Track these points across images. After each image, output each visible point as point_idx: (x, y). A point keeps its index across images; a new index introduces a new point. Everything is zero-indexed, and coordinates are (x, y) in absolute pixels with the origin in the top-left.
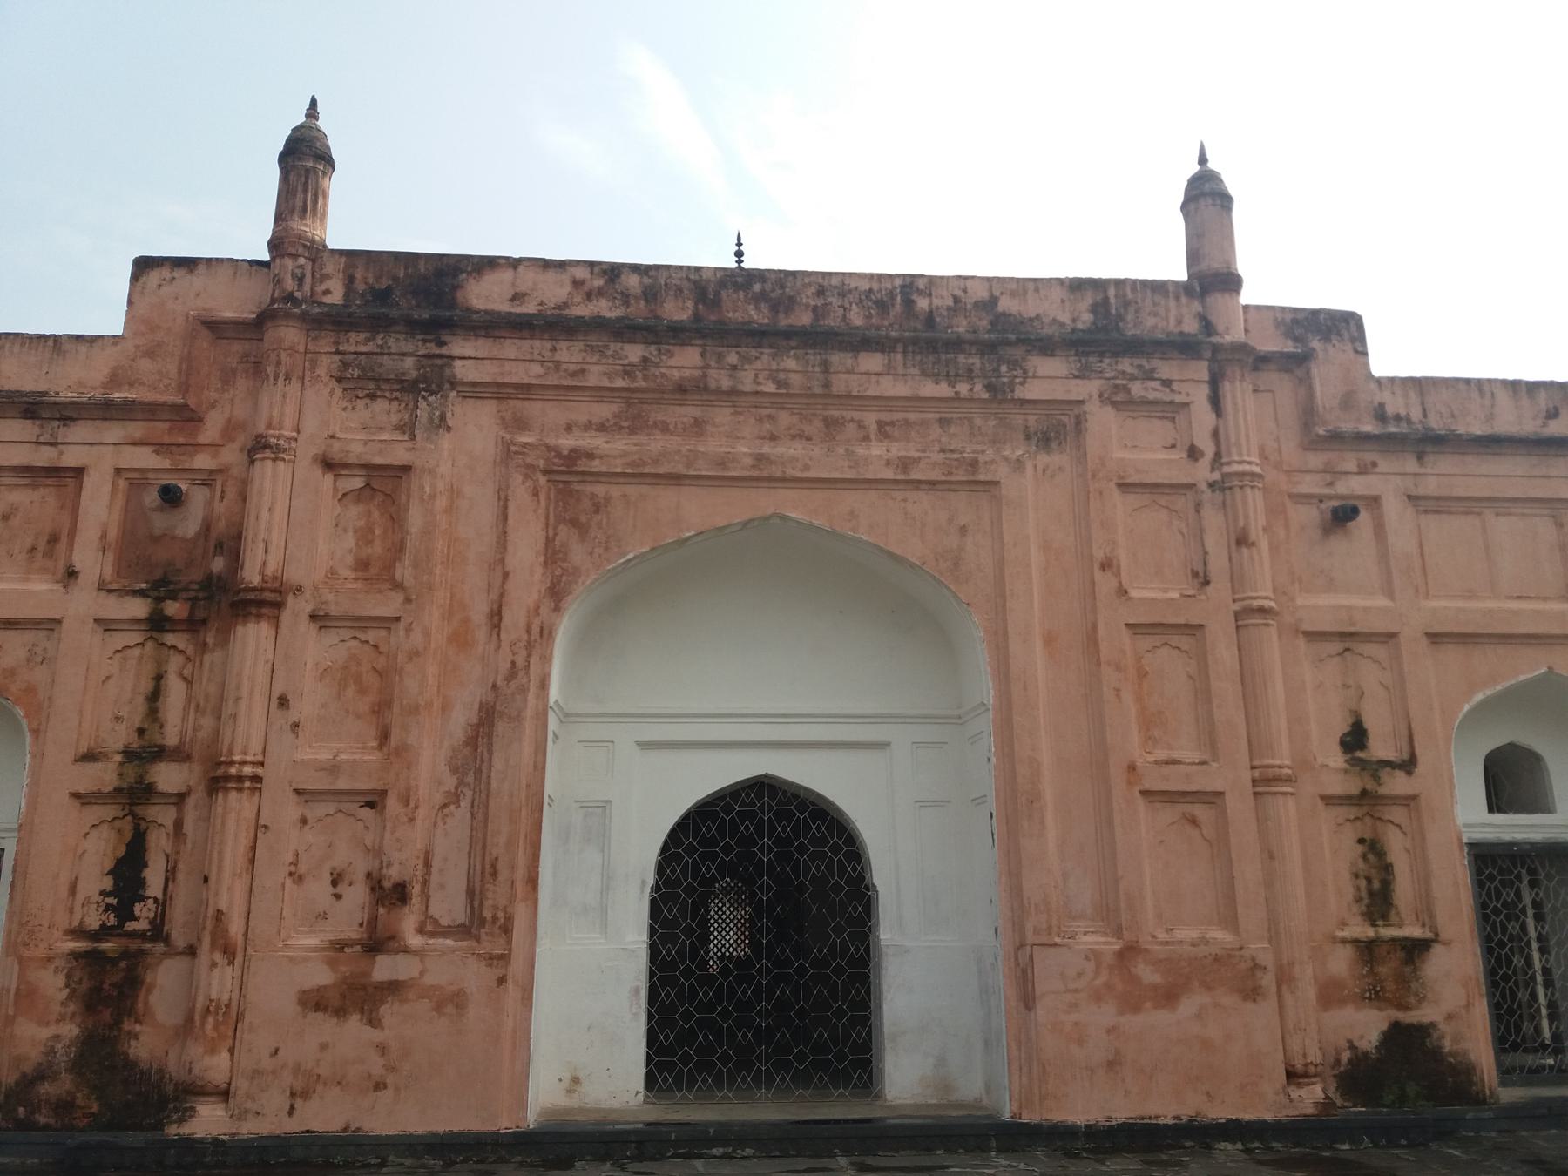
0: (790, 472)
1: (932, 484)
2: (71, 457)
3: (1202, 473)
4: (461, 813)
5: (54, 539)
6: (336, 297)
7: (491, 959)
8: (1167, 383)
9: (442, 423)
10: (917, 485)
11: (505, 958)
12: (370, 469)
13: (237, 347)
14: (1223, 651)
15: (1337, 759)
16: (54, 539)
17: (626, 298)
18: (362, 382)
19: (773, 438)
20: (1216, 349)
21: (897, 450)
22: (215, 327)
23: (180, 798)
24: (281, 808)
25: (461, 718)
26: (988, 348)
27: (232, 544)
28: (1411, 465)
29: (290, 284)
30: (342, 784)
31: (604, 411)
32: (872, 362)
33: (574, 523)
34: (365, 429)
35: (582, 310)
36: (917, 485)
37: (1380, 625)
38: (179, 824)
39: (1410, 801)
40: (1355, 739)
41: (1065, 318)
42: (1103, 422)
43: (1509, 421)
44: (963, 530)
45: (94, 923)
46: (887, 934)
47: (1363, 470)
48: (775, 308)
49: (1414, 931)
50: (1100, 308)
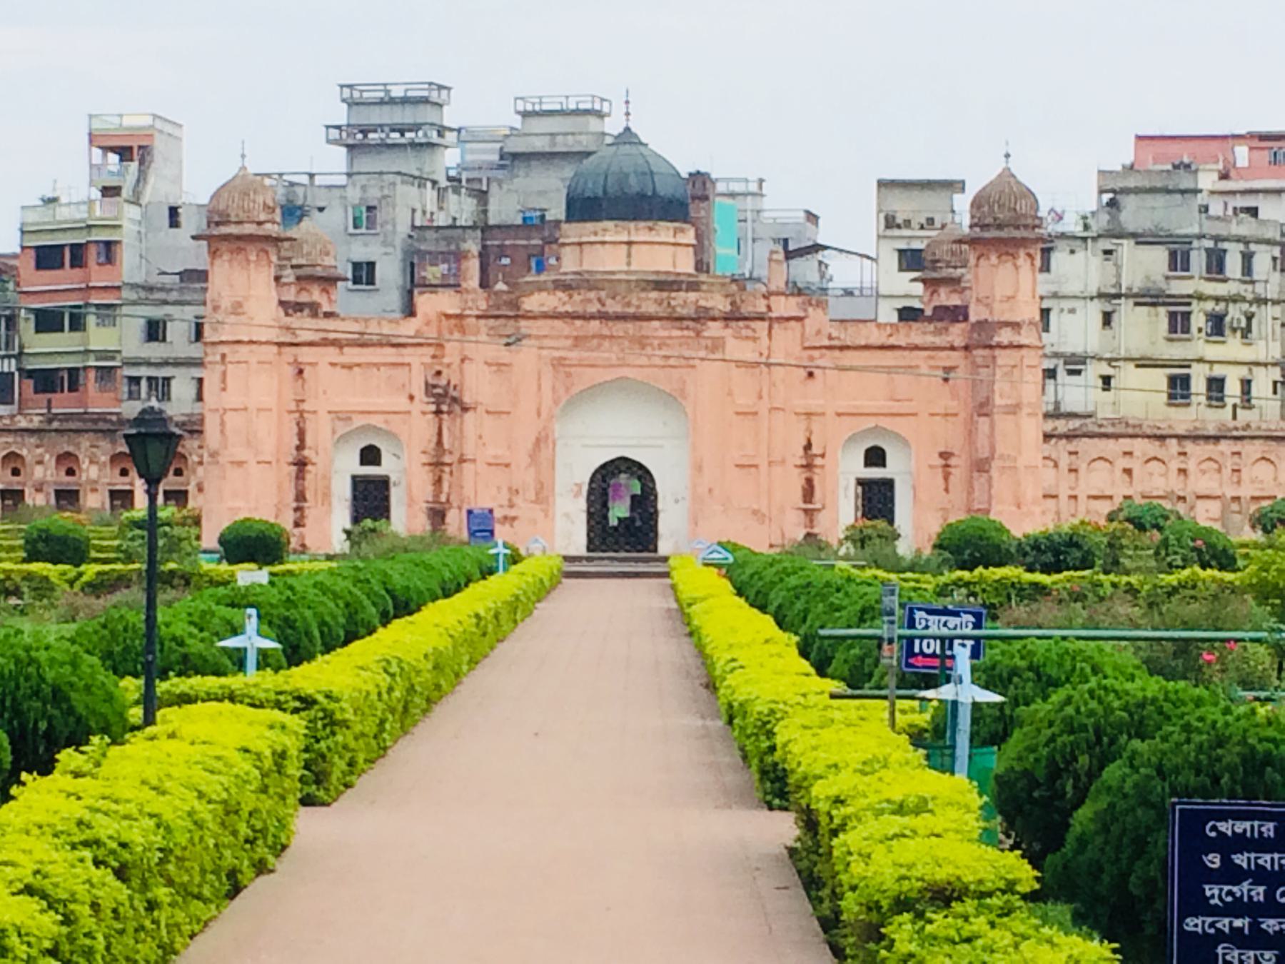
2: (406, 360)
4: (532, 470)
5: (404, 386)
7: (543, 510)
13: (453, 321)
15: (801, 452)
16: (404, 386)
18: (494, 334)
20: (771, 319)
22: (448, 316)
23: (450, 465)
24: (481, 466)
26: (693, 320)
28: (837, 353)
31: (569, 342)
32: (656, 324)
34: (496, 351)
35: (562, 309)
37: (820, 410)
38: (451, 473)
39: (822, 467)
40: (808, 446)
41: (721, 307)
46: (660, 506)
49: (818, 506)
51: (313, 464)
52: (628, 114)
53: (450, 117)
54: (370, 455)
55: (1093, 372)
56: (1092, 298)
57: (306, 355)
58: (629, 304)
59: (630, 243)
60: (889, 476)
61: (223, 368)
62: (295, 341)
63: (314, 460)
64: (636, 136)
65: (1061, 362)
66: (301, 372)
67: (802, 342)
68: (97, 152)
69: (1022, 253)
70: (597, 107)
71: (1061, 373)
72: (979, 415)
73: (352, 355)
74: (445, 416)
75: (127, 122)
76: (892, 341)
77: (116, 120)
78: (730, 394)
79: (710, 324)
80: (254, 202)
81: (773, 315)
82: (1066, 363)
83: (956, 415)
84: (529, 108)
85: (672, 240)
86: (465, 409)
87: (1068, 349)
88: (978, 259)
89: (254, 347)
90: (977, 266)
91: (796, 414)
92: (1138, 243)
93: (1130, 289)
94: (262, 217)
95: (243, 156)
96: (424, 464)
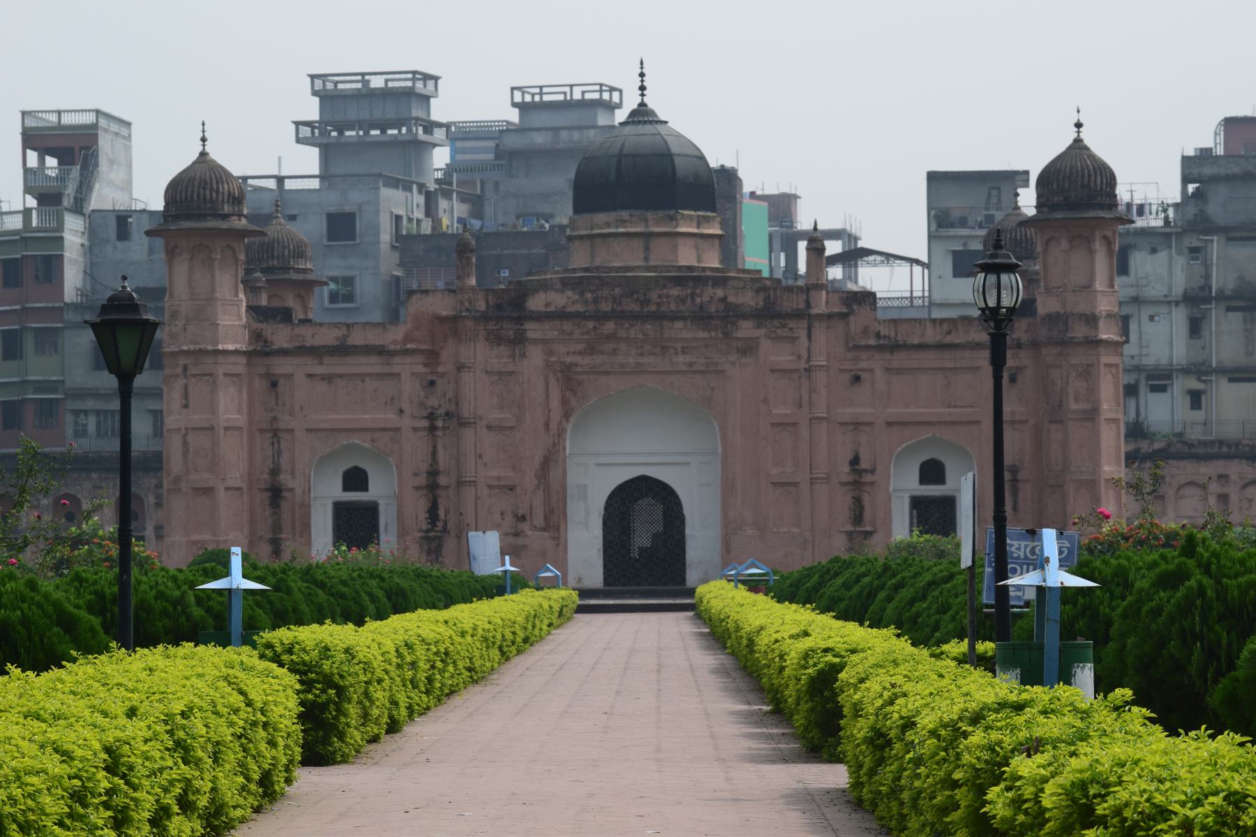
0: (649, 369)
1: (701, 372)
2: (396, 369)
3: (802, 365)
4: (540, 493)
6: (483, 308)
8: (791, 329)
9: (523, 355)
10: (696, 372)
11: (558, 538)
12: (500, 373)
14: (805, 433)
15: (846, 468)
16: (392, 399)
17: (586, 302)
18: (495, 339)
19: (642, 355)
20: (810, 315)
21: (689, 358)
22: (441, 319)
25: (538, 460)
27: (456, 400)
28: (888, 356)
29: (467, 304)
30: (502, 483)
32: (679, 324)
33: (571, 390)
34: (496, 358)
36: (696, 372)
40: (855, 461)
41: (753, 304)
42: (765, 344)
43: (931, 335)
44: (713, 389)
45: (425, 527)
46: (688, 531)
47: (869, 359)
48: (642, 305)
49: (869, 529)
50: (767, 299)
51: (291, 490)
52: (642, 88)
53: (440, 111)
54: (356, 479)
55: (1179, 386)
56: (1177, 303)
57: (282, 366)
58: (646, 302)
59: (648, 236)
60: (949, 493)
61: (184, 381)
62: (267, 349)
63: (290, 485)
64: (652, 113)
65: (1143, 376)
66: (274, 385)
67: (847, 342)
68: (33, 158)
69: (1098, 236)
70: (606, 96)
71: (1143, 388)
72: (1052, 422)
73: (331, 366)
74: (440, 433)
75: (67, 120)
76: (949, 339)
77: (53, 118)
78: (765, 401)
79: (745, 324)
80: (218, 191)
81: (814, 311)
82: (1149, 378)
83: (1024, 422)
84: (528, 98)
85: (695, 230)
86: (463, 424)
87: (1150, 361)
88: (1047, 244)
89: (221, 359)
90: (1045, 251)
91: (841, 424)
92: (1229, 239)
93: (1221, 291)
94: (227, 209)
95: (204, 140)
96: (417, 488)
